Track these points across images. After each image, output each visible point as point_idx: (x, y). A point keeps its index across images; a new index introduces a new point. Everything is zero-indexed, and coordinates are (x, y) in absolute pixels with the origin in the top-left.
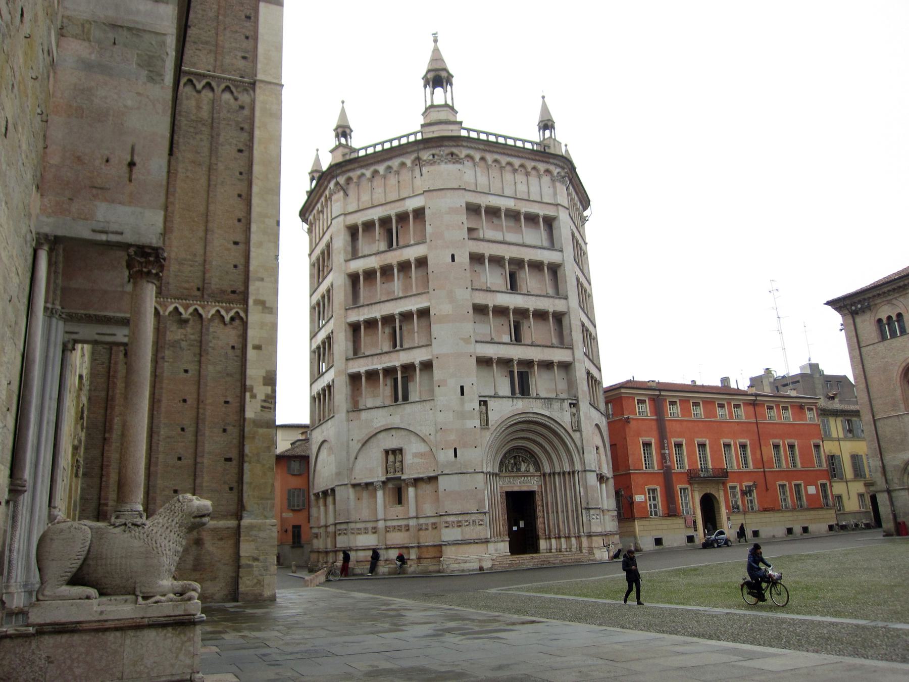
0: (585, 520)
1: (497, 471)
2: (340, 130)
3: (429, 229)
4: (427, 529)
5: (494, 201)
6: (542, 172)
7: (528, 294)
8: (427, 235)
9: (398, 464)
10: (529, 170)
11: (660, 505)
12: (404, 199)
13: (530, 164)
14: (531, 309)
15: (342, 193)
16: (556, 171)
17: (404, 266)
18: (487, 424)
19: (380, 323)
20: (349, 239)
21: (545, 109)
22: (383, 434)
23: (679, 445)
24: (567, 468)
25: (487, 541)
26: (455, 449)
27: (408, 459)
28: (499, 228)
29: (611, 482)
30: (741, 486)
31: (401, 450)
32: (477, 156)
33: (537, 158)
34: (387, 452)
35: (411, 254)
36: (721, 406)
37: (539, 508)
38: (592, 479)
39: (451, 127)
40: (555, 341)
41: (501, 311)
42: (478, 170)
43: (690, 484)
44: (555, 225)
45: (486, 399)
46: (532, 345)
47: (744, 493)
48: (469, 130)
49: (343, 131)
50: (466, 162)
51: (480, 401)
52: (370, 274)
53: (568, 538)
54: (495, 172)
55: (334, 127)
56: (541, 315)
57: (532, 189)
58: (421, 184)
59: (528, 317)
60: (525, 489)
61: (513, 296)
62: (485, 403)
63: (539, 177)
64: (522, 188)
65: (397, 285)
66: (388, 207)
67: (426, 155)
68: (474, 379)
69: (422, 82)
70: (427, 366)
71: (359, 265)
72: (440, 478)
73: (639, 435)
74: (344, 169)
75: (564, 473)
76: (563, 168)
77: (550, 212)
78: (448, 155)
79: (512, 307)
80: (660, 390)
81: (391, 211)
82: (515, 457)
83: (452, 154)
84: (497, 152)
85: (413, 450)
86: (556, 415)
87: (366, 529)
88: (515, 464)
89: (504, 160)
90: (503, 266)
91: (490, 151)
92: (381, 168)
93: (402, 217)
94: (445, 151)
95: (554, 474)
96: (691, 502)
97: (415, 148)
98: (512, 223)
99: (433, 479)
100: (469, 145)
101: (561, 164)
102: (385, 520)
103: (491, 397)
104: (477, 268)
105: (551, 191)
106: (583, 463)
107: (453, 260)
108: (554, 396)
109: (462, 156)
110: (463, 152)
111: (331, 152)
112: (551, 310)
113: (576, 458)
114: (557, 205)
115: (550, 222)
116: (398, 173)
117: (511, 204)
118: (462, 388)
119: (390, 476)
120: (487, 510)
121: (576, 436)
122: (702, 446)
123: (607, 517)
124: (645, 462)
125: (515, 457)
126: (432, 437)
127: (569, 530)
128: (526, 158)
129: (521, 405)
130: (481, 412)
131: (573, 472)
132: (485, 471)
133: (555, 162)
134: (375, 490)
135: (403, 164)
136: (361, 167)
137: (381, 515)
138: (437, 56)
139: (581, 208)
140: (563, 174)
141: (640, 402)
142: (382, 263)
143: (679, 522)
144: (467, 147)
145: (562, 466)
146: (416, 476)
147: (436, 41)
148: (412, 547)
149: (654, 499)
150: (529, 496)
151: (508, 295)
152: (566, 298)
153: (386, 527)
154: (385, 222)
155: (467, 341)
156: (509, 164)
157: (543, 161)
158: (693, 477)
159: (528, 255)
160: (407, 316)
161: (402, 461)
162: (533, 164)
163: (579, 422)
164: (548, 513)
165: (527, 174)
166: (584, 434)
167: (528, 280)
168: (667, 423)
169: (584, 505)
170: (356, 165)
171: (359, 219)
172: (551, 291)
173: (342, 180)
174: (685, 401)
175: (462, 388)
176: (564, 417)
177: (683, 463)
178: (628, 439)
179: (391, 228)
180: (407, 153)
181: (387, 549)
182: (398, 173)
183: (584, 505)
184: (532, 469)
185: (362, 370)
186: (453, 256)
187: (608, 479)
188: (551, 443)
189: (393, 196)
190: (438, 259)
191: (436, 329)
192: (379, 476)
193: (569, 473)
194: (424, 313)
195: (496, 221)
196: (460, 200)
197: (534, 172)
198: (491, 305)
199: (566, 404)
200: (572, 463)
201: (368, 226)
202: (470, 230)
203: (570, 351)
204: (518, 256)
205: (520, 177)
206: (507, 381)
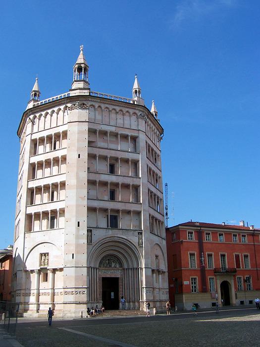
6: (131, 114)
11: (198, 287)
13: (125, 110)
14: (120, 183)
17: (56, 161)
20: (33, 146)
23: (210, 255)
24: (135, 266)
26: (73, 254)
27: (51, 257)
28: (106, 141)
29: (167, 274)
30: (244, 277)
31: (48, 254)
33: (129, 107)
34: (41, 255)
35: (59, 154)
36: (235, 236)
37: (120, 287)
41: (104, 184)
43: (215, 276)
45: (91, 229)
47: (245, 281)
53: (134, 302)
54: (106, 113)
57: (126, 122)
60: (113, 276)
64: (120, 122)
68: (85, 218)
70: (62, 211)
71: (35, 159)
73: (188, 250)
76: (143, 112)
77: (135, 134)
79: (109, 182)
81: (52, 132)
83: (84, 104)
88: (109, 263)
89: (111, 107)
95: (129, 269)
96: (216, 284)
98: (114, 139)
99: (61, 270)
105: (136, 122)
107: (79, 157)
110: (90, 103)
115: (134, 139)
117: (113, 129)
118: (79, 222)
119: (42, 267)
122: (223, 256)
123: (161, 292)
124: (190, 263)
127: (135, 299)
129: (111, 233)
140: (143, 115)
141: (189, 233)
143: (207, 295)
144: (91, 101)
145: (133, 264)
149: (195, 284)
150: (116, 280)
154: (49, 138)
155: (83, 199)
158: (216, 271)
162: (127, 109)
164: (125, 289)
165: (123, 115)
167: (120, 169)
168: (204, 244)
171: (37, 136)
173: (32, 117)
174: (214, 233)
175: (79, 222)
176: (134, 239)
177: (212, 264)
178: (182, 252)
179: (54, 140)
184: (118, 266)
187: (165, 272)
190: (72, 157)
192: (37, 267)
193: (136, 269)
197: (127, 114)
199: (136, 233)
201: (42, 140)
202: (89, 142)
205: (120, 116)
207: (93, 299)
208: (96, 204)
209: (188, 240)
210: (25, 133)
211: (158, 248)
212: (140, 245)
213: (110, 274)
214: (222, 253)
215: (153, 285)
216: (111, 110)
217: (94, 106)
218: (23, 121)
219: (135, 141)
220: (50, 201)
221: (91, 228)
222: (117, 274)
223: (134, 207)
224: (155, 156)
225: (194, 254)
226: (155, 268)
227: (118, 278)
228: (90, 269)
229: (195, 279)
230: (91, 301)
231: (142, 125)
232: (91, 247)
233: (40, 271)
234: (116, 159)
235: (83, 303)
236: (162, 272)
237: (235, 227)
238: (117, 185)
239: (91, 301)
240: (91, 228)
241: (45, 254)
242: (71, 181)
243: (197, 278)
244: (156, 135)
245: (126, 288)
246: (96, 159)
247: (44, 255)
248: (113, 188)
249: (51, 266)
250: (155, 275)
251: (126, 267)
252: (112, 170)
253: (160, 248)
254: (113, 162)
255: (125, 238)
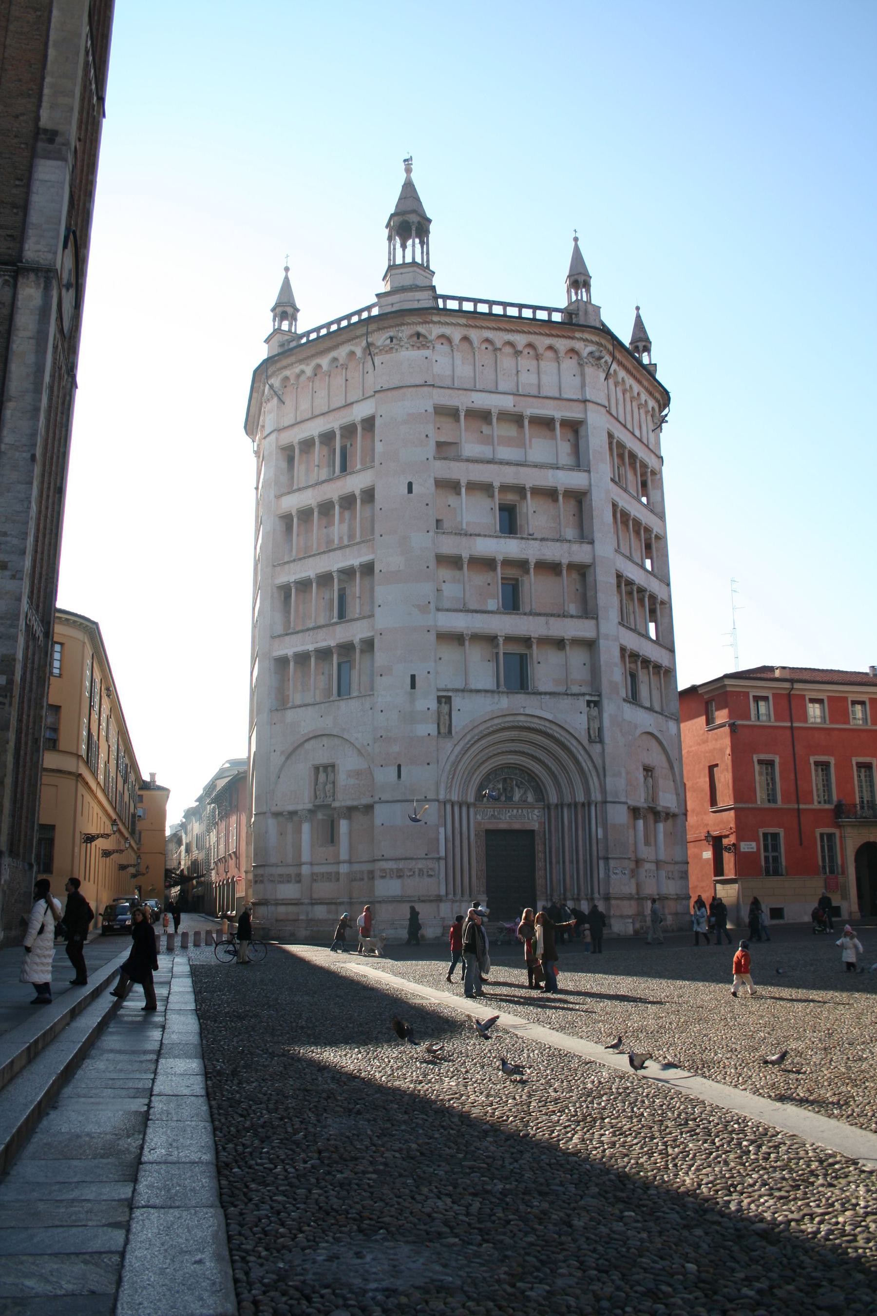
0: (602, 875)
1: (471, 799)
2: (279, 310)
3: (379, 447)
4: (362, 879)
5: (481, 401)
6: (562, 354)
7: (531, 537)
8: (377, 456)
9: (329, 787)
10: (541, 350)
12: (352, 403)
13: (542, 342)
15: (275, 400)
16: (586, 350)
17: (348, 501)
18: (450, 732)
19: (314, 585)
20: (284, 465)
21: (577, 259)
22: (312, 742)
24: (581, 798)
25: (439, 899)
26: (399, 766)
27: (342, 779)
32: (456, 334)
33: (554, 332)
34: (317, 769)
35: (355, 483)
38: (619, 815)
39: (419, 295)
40: (572, 609)
41: (487, 564)
42: (458, 356)
43: (839, 826)
44: (582, 432)
45: (450, 694)
46: (531, 614)
48: (445, 298)
49: (285, 308)
50: (438, 346)
51: (439, 699)
52: (305, 514)
55: (273, 304)
56: (552, 568)
57: (545, 379)
58: (373, 381)
59: (527, 572)
60: (517, 826)
61: (502, 540)
62: (448, 699)
63: (557, 360)
64: (528, 379)
65: (338, 530)
66: (331, 417)
67: (380, 339)
69: (386, 232)
70: (369, 645)
72: (378, 808)
74: (279, 365)
75: (576, 805)
76: (597, 344)
77: (573, 413)
78: (411, 336)
79: (499, 558)
80: (792, 681)
81: (335, 423)
82: (505, 780)
83: (418, 335)
84: (488, 328)
85: (348, 763)
86: (560, 718)
87: (289, 876)
88: (505, 789)
89: (499, 338)
90: (492, 496)
91: (476, 327)
92: (325, 362)
93: (349, 430)
94: (405, 332)
97: (363, 330)
99: (369, 809)
100: (443, 319)
101: (595, 338)
102: (311, 864)
103: (457, 690)
104: (452, 500)
105: (578, 379)
106: (603, 790)
107: (410, 490)
108: (561, 689)
109: (433, 337)
111: (267, 341)
112: (565, 561)
113: (594, 782)
114: (585, 401)
115: (574, 427)
116: (345, 367)
117: (507, 403)
118: (413, 677)
120: (442, 854)
121: (596, 748)
123: (663, 873)
125: (505, 780)
126: (369, 748)
128: (535, 333)
129: (504, 703)
130: (439, 713)
131: (589, 804)
132: (442, 797)
133: (586, 336)
134: (300, 823)
135: (352, 353)
136: (301, 361)
137: (306, 857)
138: (409, 192)
139: (652, 403)
140: (597, 354)
141: (757, 699)
142: (319, 499)
144: (439, 322)
146: (349, 803)
147: (408, 170)
148: (341, 903)
151: (495, 540)
152: (592, 542)
153: (313, 874)
154: (327, 438)
155: (424, 609)
156: (510, 344)
157: (564, 337)
159: (531, 478)
160: (348, 573)
161: (334, 783)
162: (548, 341)
163: (600, 730)
164: (551, 863)
165: (538, 357)
166: (606, 747)
167: (535, 515)
169: (601, 854)
170: (293, 359)
172: (570, 533)
173: (276, 381)
175: (413, 677)
180: (357, 337)
181: (313, 904)
182: (345, 367)
183: (601, 854)
184: (530, 798)
185: (290, 652)
186: (410, 485)
188: (556, 759)
189: (339, 401)
190: (390, 491)
191: (380, 592)
192: (304, 803)
193: (583, 804)
194: (368, 569)
195: (486, 429)
196: (425, 402)
197: (550, 354)
198: (465, 555)
199: (582, 703)
200: (587, 791)
201: (307, 445)
202: (440, 445)
203: (593, 622)
204: (515, 482)
205: (526, 363)
206: (490, 667)
207: (459, 891)
208: (460, 623)
209: (753, 721)
210: (263, 426)
211: (654, 743)
212: (597, 737)
213: (508, 819)
214: (861, 759)
215: (635, 851)
216: (499, 345)
217: (449, 340)
218: (255, 395)
219: (576, 432)
220: (335, 620)
221: (448, 690)
222: (532, 819)
223: (575, 628)
224: (643, 474)
225: (770, 763)
226: (640, 800)
227: (533, 831)
228: (449, 807)
229: (775, 836)
230: (451, 896)
231: (597, 385)
232: (448, 745)
233: (312, 812)
234: (520, 490)
235: (431, 901)
236: (667, 814)
237: (836, 678)
238: (522, 565)
239: (451, 896)
240: (448, 690)
241: (326, 767)
242: (388, 560)
243: (782, 835)
244: (647, 412)
245: (554, 860)
246: (459, 493)
247: (329, 768)
248: (512, 572)
249: (342, 801)
250: (640, 823)
251: (553, 799)
252: (510, 522)
253: (660, 743)
254: (511, 498)
255: (549, 717)
